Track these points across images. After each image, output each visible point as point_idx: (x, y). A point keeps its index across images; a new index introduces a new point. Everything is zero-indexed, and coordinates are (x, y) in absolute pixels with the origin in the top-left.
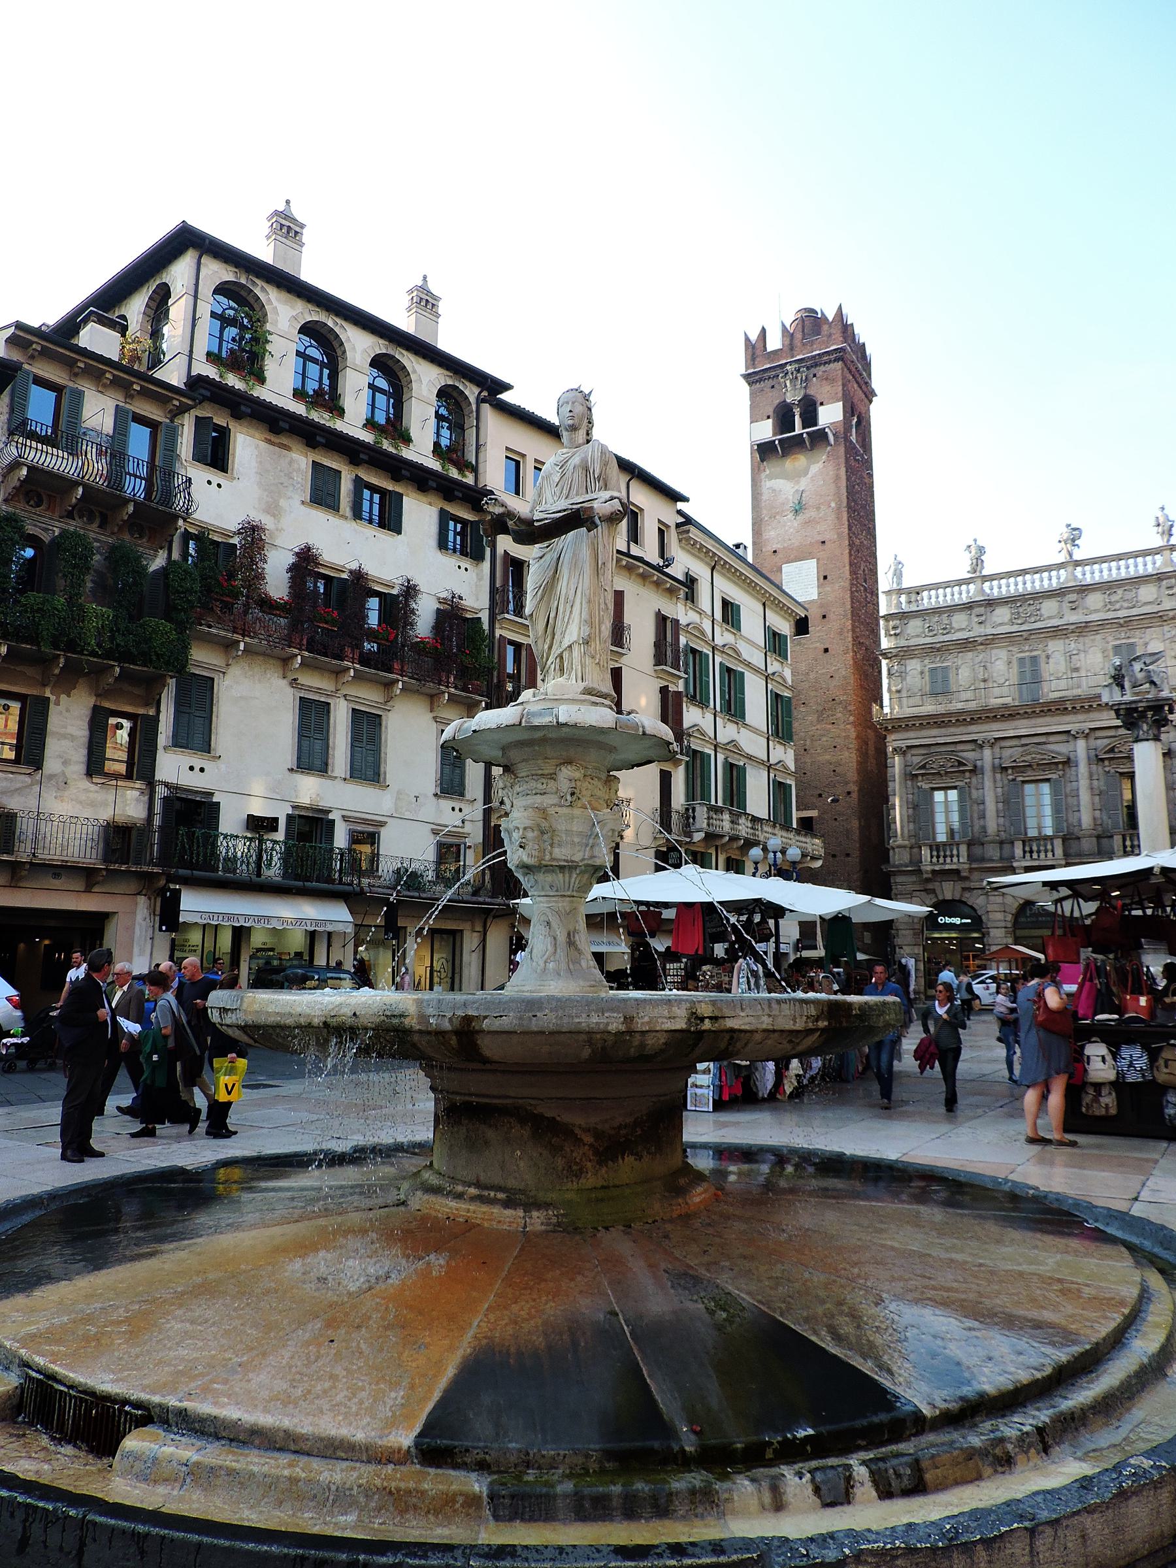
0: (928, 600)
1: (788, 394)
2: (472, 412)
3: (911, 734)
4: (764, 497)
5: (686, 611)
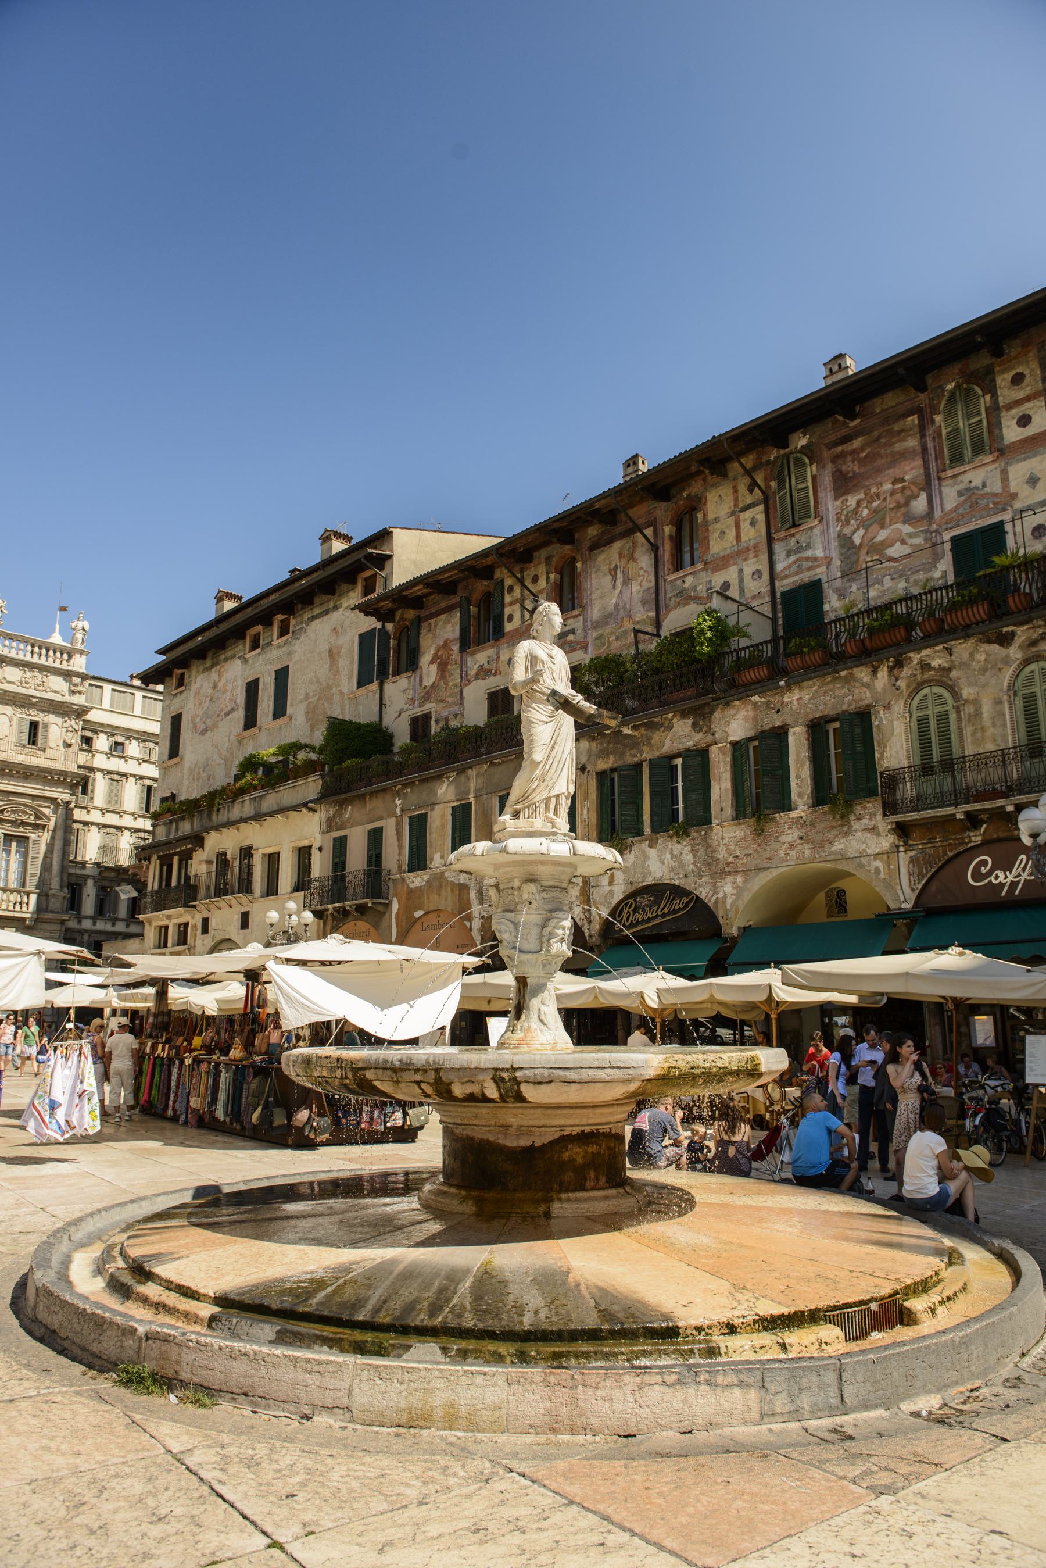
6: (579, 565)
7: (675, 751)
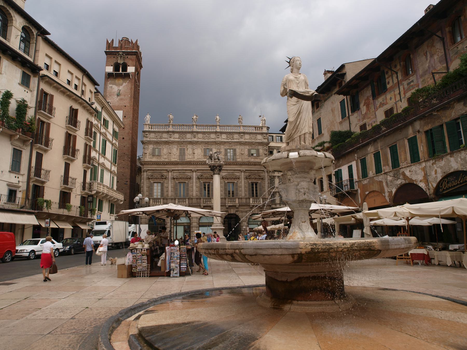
1: (119, 61)
2: (34, 38)
5: (95, 120)
6: (411, 56)
7: (457, 117)
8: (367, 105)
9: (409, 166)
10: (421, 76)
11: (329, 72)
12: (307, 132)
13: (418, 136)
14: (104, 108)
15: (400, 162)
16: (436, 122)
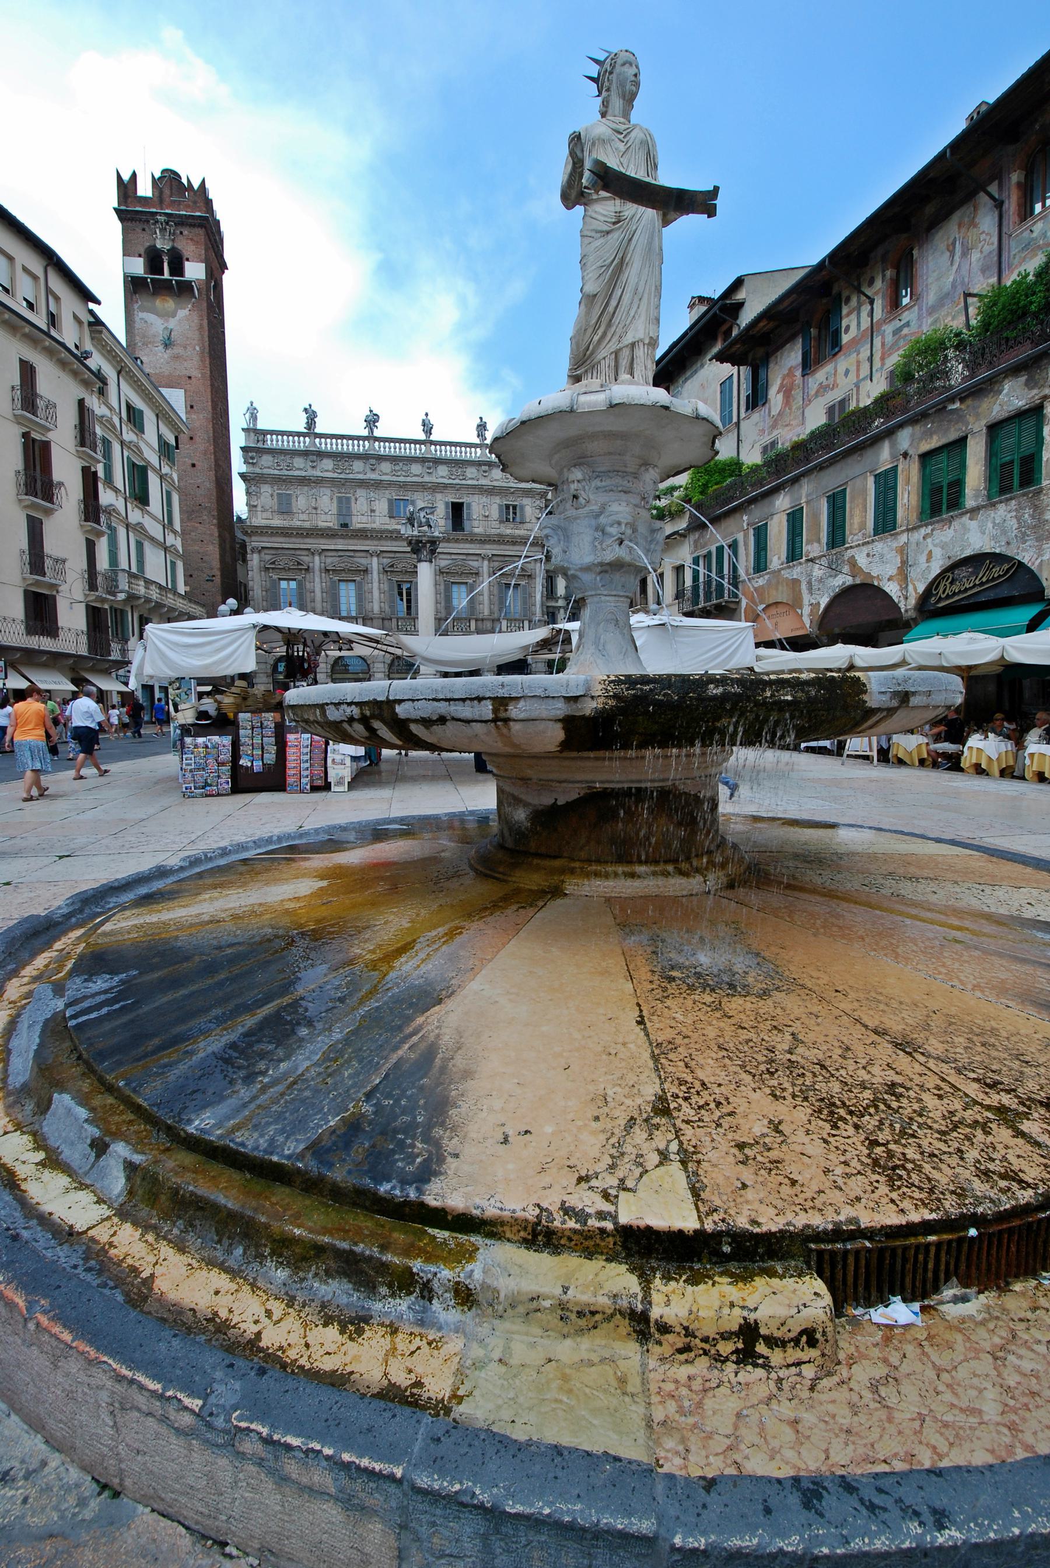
0: (272, 442)
3: (265, 539)
4: (137, 326)
6: (915, 252)
8: (787, 392)
9: (868, 543)
10: (932, 310)
11: (702, 299)
12: (642, 337)
13: (900, 468)
14: (123, 373)
15: (847, 532)
16: (952, 429)
